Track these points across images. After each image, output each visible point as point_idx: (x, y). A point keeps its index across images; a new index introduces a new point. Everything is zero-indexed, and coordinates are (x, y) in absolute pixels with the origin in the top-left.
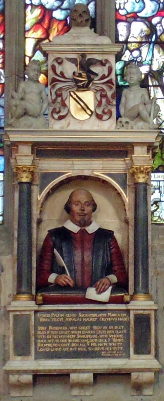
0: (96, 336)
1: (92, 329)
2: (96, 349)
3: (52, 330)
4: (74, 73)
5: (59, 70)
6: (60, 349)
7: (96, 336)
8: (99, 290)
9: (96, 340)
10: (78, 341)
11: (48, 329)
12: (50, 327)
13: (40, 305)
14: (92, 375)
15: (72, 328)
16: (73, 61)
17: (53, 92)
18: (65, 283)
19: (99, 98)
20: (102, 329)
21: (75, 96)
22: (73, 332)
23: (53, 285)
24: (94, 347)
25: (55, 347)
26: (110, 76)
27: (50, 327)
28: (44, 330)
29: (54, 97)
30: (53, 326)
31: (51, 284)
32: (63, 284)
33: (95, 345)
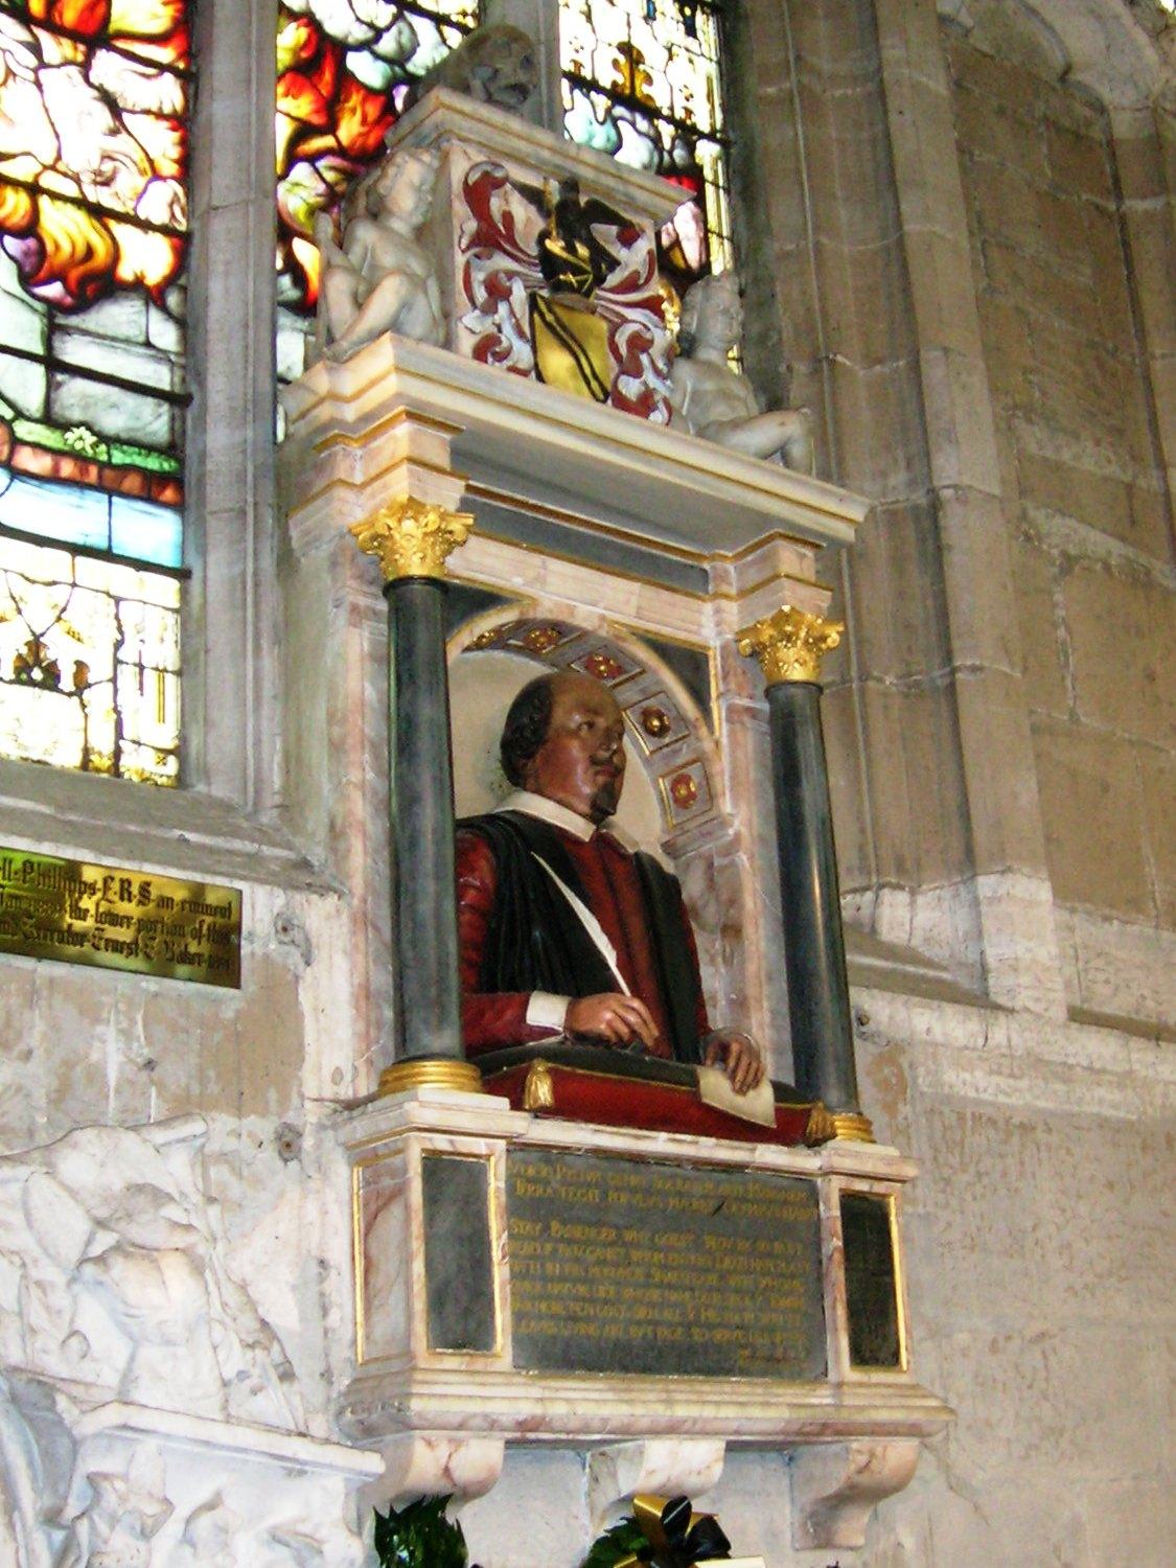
0: (713, 1279)
1: (698, 1246)
2: (719, 1335)
3: (562, 1240)
4: (544, 235)
5: (496, 205)
6: (592, 1330)
7: (713, 1279)
8: (740, 1076)
9: (716, 1298)
10: (655, 1295)
11: (547, 1228)
12: (555, 1225)
13: (541, 1113)
14: (719, 1445)
15: (629, 1236)
16: (534, 196)
17: (479, 277)
18: (624, 1030)
19: (623, 350)
20: (733, 1251)
21: (549, 318)
22: (636, 1255)
23: (553, 1040)
24: (710, 1327)
25: (573, 1318)
26: (545, 330)
27: (555, 1225)
28: (534, 1239)
29: (481, 294)
30: (564, 1223)
31: (548, 1032)
32: (616, 1033)
33: (712, 1315)
